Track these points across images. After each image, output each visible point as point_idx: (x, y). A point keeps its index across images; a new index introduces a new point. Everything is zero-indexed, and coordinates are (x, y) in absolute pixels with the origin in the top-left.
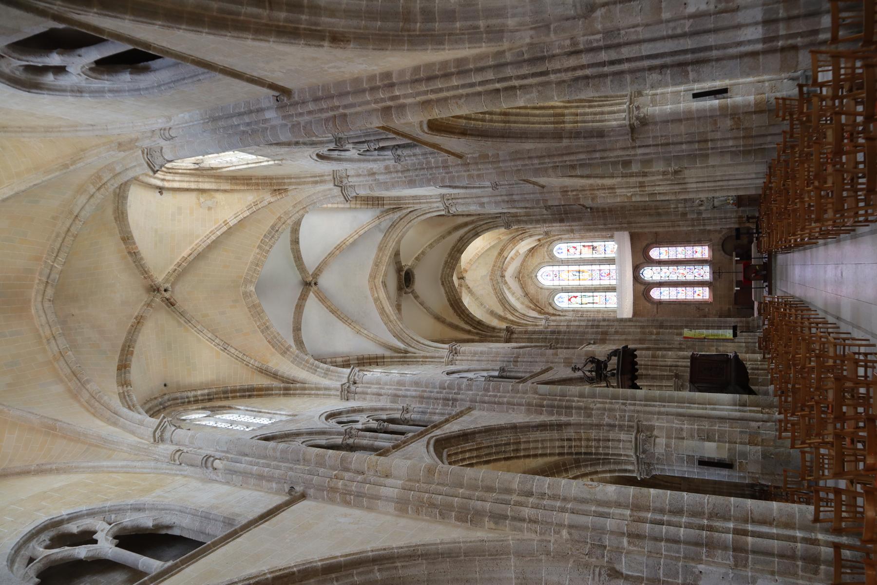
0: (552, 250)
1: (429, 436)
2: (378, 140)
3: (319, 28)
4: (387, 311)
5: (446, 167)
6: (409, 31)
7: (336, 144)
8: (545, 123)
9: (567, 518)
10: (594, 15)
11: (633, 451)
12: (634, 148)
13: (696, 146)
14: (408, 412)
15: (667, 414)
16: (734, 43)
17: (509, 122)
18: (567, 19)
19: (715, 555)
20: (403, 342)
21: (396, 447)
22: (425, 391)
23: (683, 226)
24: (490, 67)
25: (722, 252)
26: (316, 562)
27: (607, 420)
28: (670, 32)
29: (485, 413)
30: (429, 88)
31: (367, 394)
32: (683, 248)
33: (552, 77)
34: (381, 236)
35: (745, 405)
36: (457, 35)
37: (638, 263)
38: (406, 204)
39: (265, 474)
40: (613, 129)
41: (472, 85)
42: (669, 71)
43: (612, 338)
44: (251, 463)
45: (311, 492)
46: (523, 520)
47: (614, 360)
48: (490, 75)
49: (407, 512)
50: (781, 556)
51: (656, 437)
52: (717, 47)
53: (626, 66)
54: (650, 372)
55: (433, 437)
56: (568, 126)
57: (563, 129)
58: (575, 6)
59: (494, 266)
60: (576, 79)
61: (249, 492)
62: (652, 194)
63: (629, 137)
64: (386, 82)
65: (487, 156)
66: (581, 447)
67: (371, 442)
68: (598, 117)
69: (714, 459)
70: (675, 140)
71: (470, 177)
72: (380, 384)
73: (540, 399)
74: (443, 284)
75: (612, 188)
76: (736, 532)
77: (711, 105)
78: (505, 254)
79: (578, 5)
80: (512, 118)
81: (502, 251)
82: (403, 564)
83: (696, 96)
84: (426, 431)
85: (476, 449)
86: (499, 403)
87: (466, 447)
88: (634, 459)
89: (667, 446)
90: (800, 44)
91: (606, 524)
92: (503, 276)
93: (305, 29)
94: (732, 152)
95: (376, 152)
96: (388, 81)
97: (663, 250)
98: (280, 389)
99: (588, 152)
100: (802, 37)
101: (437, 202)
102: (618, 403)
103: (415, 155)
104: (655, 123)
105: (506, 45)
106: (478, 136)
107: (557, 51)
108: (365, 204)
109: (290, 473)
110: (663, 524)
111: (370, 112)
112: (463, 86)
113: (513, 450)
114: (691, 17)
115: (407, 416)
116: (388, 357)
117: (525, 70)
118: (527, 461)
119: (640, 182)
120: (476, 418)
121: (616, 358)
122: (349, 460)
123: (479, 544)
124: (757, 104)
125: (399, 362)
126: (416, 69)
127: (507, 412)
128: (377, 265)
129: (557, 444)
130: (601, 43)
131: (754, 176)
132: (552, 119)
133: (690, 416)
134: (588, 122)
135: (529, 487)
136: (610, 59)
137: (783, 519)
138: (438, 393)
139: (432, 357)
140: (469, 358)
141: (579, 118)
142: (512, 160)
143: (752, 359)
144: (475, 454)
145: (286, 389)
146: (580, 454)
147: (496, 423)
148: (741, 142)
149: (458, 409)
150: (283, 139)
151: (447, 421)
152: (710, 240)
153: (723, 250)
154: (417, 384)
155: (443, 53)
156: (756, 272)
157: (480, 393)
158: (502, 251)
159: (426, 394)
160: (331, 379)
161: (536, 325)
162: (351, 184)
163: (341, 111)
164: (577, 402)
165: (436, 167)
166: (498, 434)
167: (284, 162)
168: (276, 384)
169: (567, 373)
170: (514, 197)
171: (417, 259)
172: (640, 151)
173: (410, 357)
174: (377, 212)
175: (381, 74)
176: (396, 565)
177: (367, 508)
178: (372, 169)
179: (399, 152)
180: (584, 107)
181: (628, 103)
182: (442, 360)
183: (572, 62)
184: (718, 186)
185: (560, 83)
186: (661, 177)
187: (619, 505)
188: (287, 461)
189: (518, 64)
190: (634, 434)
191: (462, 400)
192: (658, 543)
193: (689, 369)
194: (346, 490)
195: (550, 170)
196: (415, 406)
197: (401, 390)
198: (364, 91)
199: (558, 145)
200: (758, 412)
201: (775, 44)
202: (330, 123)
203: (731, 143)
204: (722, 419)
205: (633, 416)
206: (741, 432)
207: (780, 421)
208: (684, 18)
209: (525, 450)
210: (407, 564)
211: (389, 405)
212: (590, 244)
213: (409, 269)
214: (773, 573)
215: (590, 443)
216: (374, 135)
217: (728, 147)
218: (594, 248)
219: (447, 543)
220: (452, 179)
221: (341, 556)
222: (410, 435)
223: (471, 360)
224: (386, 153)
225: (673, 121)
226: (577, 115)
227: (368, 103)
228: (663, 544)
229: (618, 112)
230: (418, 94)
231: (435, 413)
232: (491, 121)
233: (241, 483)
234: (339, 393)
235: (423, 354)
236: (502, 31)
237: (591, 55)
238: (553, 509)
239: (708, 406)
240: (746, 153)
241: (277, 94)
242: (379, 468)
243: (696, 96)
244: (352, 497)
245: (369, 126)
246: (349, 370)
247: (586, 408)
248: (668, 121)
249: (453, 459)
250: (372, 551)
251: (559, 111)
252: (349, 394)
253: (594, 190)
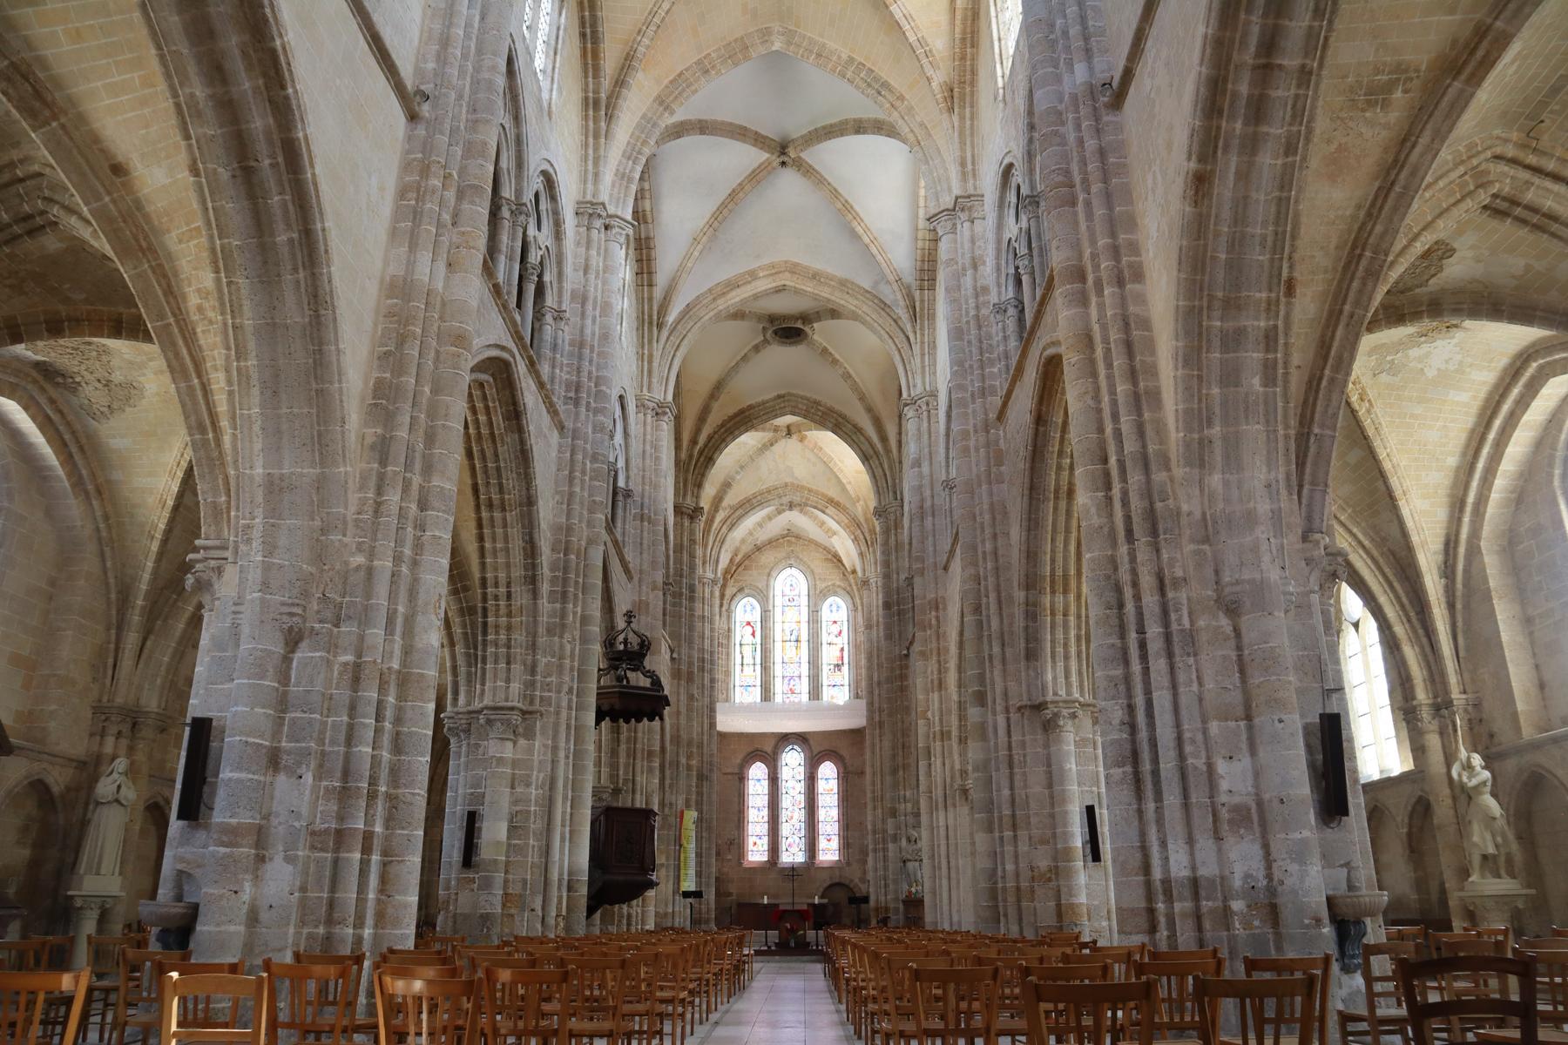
0: (835, 594)
1: (515, 350)
2: (1032, 273)
3: (1220, 152)
4: (733, 293)
5: (983, 392)
6: (1209, 308)
7: (1027, 196)
8: (1053, 561)
9: (385, 564)
10: (1221, 614)
11: (491, 704)
12: (1007, 710)
13: (1007, 812)
14: (555, 319)
16: (1165, 836)
17: (1057, 498)
18: (1217, 572)
19: (329, 800)
20: (678, 321)
21: (497, 290)
22: (592, 351)
23: (874, 816)
24: (1144, 446)
25: (828, 883)
26: (304, 129)
27: (543, 661)
28: (1187, 735)
29: (554, 454)
30: (1112, 346)
31: (588, 248)
32: (836, 818)
33: (1123, 549)
34: (866, 284)
35: (570, 889)
36: (1199, 391)
37: (811, 742)
38: (922, 329)
39: (450, 50)
40: (1040, 674)
41: (1115, 417)
42: (1125, 736)
43: (682, 690)
44: (468, 25)
45: (421, 131)
46: (379, 491)
47: (645, 682)
48: (1130, 446)
49: (388, 297)
50: (331, 904)
51: (515, 743)
52: (1159, 810)
53: (1136, 667)
54: (623, 747)
56: (1047, 600)
57: (1041, 592)
58: (1237, 583)
59: (810, 490)
60: (1118, 590)
61: (418, 20)
62: (929, 752)
63: (1024, 703)
64: (1126, 274)
65: (999, 463)
66: (497, 616)
67: (504, 249)
68: (1060, 650)
69: (479, 838)
70: (1017, 777)
71: (965, 435)
72: (604, 272)
73: (579, 550)
74: (779, 397)
75: (941, 685)
76: (368, 837)
77: (1073, 835)
78: (831, 510)
79: (1238, 588)
80: (1063, 504)
81: (837, 505)
82: (302, 282)
83: (1090, 811)
84: (524, 347)
85: (492, 434)
86: (571, 479)
87: (497, 415)
88: (477, 705)
89: (500, 761)
90: (1158, 935)
91: (375, 627)
92: (791, 506)
93: (1219, 128)
94: (995, 870)
95: (1012, 271)
96: (1127, 275)
97: (833, 785)
98: (596, 92)
99: (1002, 634)
100: (1169, 937)
101: (924, 383)
102: (573, 680)
103: (1005, 338)
104: (1047, 746)
105: (1179, 472)
106: (1035, 446)
107: (1165, 556)
108: (923, 255)
109: (453, 95)
110: (377, 721)
111: (1077, 247)
112: (1114, 403)
113: (490, 499)
114: (1210, 766)
115: (549, 318)
116: (650, 293)
117: (1136, 504)
118: (472, 525)
119: (949, 732)
120: (545, 436)
121: (648, 686)
122: (477, 200)
123: (338, 414)
124: (1072, 906)
125: (643, 313)
126: (1146, 324)
127: (557, 492)
128: (815, 276)
129: (502, 575)
130: (1174, 627)
131: (955, 919)
132: (1059, 572)
133: (550, 796)
134: (1053, 633)
135: (436, 504)
136: (1148, 642)
137: (390, 910)
138: (590, 373)
139: (650, 372)
140: (648, 437)
141: (1059, 618)
142: (992, 504)
143: (648, 911)
144: (485, 431)
145: (596, 103)
146: (485, 615)
147: (537, 470)
148: (1011, 884)
149: (561, 407)
150: (1038, 95)
151: (541, 385)
152: (848, 864)
153: (831, 886)
154: (605, 337)
155: (1171, 366)
156: (792, 931)
157: (588, 446)
158: (837, 505)
159: (587, 351)
160: (613, 185)
161: (704, 563)
162: (959, 226)
163: (1081, 197)
164: (574, 611)
165: (983, 375)
166: (519, 474)
167: (1001, 105)
168: (606, 83)
169: (622, 604)
170: (930, 518)
171: (825, 351)
172: (1001, 720)
173: (650, 331)
174: (909, 277)
175: (1140, 264)
176: (301, 270)
177: (395, 228)
178: (984, 263)
179: (1011, 311)
180: (1079, 627)
181: (1082, 699)
182: (645, 389)
183: (1147, 581)
184: (939, 862)
185: (1113, 563)
186: (957, 767)
187: (408, 651)
188: (474, 92)
189: (1148, 493)
190: (520, 705)
191: (577, 414)
192: (345, 711)
193: (629, 805)
194: (425, 192)
195: (973, 571)
196: (567, 334)
197: (594, 309)
198: (1113, 235)
199: (1015, 584)
200: (559, 909)
201: (1161, 897)
202: (1061, 178)
203: (1010, 867)
204: (547, 852)
205: (550, 705)
206: (525, 882)
208: (1208, 758)
209: (492, 519)
210: (303, 290)
211: (568, 286)
212: (846, 660)
213: (806, 335)
214: (303, 889)
215: (503, 632)
216: (1042, 264)
217: (1003, 864)
218: (838, 667)
219: (338, 360)
220: (963, 403)
221: (314, 175)
222: (518, 318)
224: (1011, 288)
225: (1049, 774)
226: (1065, 615)
227: (1093, 242)
228: (345, 718)
229: (1068, 685)
230: (1104, 328)
231: (553, 367)
232: (1059, 468)
233: (433, 5)
234: (589, 198)
235: (657, 354)
236: (1202, 465)
237: (1157, 610)
238: (399, 542)
239: (568, 829)
240: (993, 893)
241: (1115, 84)
242: (464, 251)
243: (1090, 811)
244: (413, 202)
245: (1054, 244)
246: (629, 218)
247: (563, 626)
248: (1049, 765)
249: (477, 393)
250: (324, 230)
251: (1073, 584)
252: (586, 217)
253: (939, 654)
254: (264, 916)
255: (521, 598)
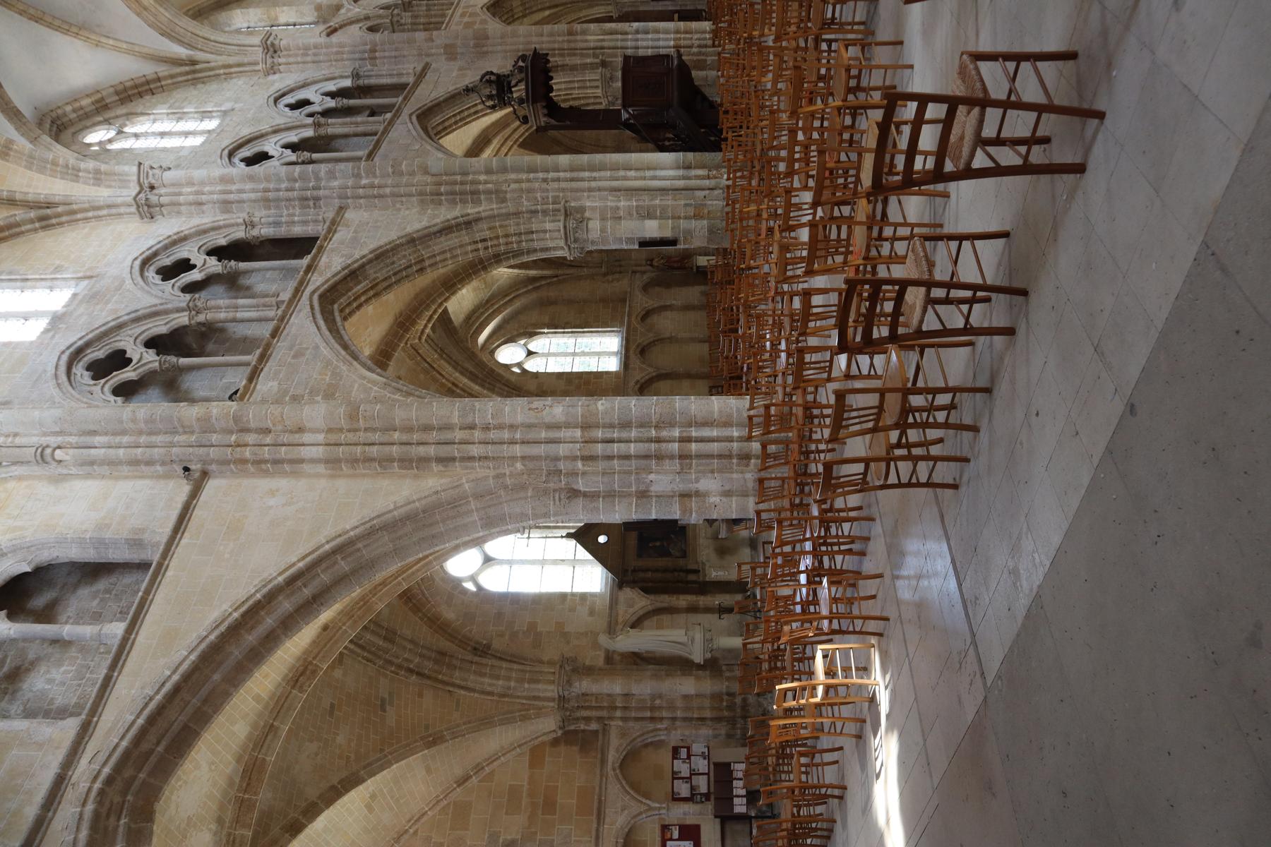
9: (518, 450)
15: (599, 189)
20: (180, 42)
27: (526, 204)
31: (180, 204)
35: (689, 167)
45: (213, 467)
50: (720, 456)
51: (589, 219)
55: (314, 292)
66: (499, 245)
85: (372, 288)
86: (381, 196)
89: (603, 230)
98: (32, 221)
102: (537, 179)
116: (166, 78)
122: (245, 419)
125: (187, 81)
129: (469, 248)
135: (471, 419)
137: (723, 419)
138: (287, 190)
139: (239, 65)
140: (299, 59)
145: (41, 219)
159: (271, 195)
160: (110, 187)
166: (393, 255)
168: (20, 214)
177: (291, 472)
182: (257, 68)
187: (568, 425)
191: (326, 197)
192: (611, 463)
196: (260, 214)
205: (558, 197)
206: (686, 205)
207: (728, 187)
211: (221, 218)
214: (712, 472)
221: (299, 561)
223: (304, 63)
228: (615, 461)
234: (133, 209)
235: (222, 60)
247: (497, 192)
252: (152, 210)
254: (727, 488)
255: (482, 231)
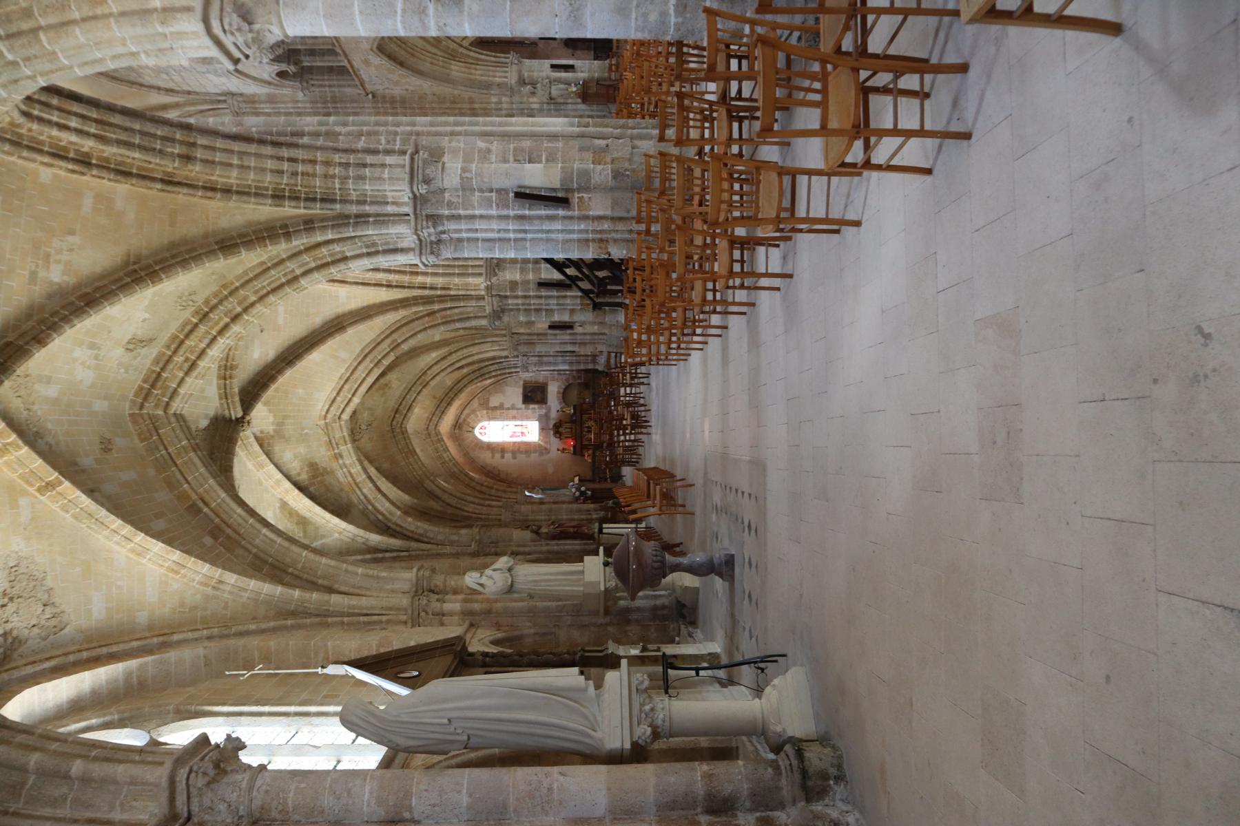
66: (314, 175)
